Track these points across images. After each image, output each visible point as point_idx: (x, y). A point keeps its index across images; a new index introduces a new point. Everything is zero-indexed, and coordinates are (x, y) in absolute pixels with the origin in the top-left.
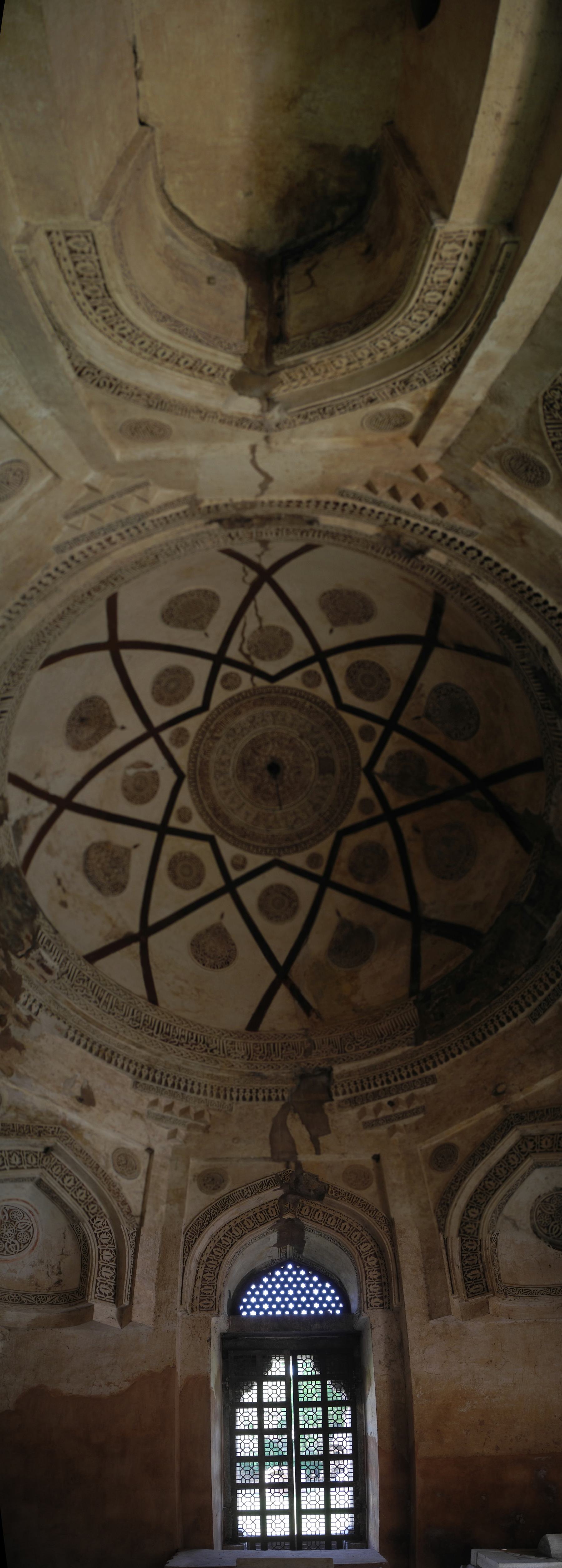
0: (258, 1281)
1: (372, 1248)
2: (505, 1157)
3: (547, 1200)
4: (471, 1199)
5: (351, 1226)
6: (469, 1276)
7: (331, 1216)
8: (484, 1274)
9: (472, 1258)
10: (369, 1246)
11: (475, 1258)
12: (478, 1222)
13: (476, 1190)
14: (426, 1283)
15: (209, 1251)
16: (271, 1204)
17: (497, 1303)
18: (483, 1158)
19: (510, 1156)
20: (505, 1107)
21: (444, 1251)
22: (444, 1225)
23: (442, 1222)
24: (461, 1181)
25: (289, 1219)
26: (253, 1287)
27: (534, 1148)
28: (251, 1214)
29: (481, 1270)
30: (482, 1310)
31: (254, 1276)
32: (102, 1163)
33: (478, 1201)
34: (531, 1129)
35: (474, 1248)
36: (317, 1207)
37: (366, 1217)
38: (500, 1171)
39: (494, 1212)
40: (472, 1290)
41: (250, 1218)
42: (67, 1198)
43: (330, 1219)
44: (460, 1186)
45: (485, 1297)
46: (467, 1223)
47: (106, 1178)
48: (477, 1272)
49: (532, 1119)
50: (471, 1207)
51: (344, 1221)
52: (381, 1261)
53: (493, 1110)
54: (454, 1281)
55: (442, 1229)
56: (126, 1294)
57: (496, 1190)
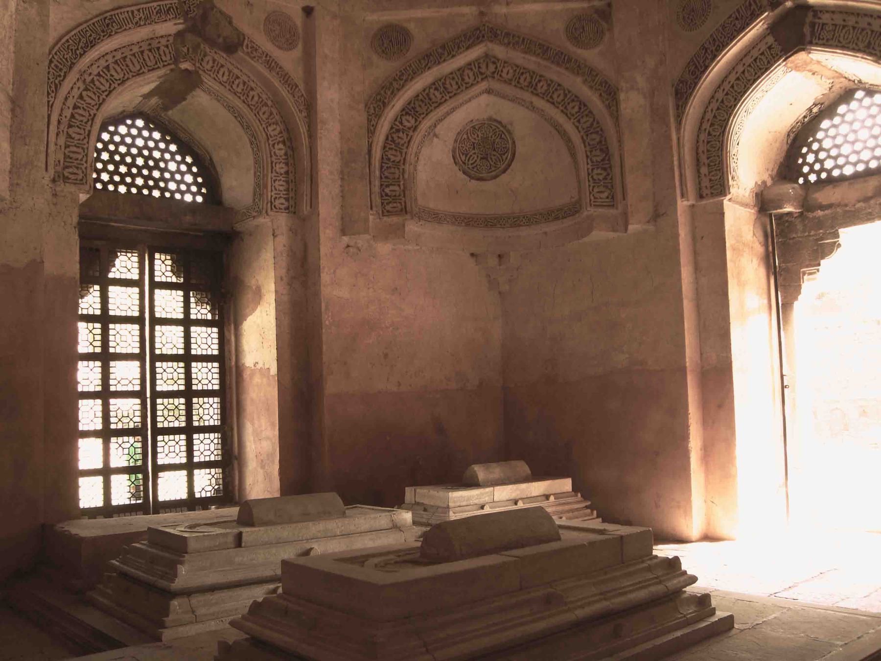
2: (461, 70)
4: (409, 104)
5: (260, 97)
6: (387, 190)
7: (238, 77)
8: (404, 191)
9: (392, 170)
11: (397, 171)
12: (411, 133)
13: (418, 96)
14: (342, 191)
16: (163, 41)
17: (412, 227)
18: (439, 63)
19: (467, 71)
22: (375, 126)
23: (373, 122)
24: (406, 81)
25: (186, 70)
27: (494, 73)
28: (136, 49)
29: (402, 187)
30: (397, 232)
33: (416, 109)
34: (499, 51)
35: (398, 159)
36: (222, 61)
37: (284, 92)
40: (388, 208)
43: (237, 82)
44: (403, 86)
48: (396, 188)
49: (506, 41)
50: (407, 113)
51: (252, 89)
52: (290, 152)
55: (371, 132)
57: (441, 104)
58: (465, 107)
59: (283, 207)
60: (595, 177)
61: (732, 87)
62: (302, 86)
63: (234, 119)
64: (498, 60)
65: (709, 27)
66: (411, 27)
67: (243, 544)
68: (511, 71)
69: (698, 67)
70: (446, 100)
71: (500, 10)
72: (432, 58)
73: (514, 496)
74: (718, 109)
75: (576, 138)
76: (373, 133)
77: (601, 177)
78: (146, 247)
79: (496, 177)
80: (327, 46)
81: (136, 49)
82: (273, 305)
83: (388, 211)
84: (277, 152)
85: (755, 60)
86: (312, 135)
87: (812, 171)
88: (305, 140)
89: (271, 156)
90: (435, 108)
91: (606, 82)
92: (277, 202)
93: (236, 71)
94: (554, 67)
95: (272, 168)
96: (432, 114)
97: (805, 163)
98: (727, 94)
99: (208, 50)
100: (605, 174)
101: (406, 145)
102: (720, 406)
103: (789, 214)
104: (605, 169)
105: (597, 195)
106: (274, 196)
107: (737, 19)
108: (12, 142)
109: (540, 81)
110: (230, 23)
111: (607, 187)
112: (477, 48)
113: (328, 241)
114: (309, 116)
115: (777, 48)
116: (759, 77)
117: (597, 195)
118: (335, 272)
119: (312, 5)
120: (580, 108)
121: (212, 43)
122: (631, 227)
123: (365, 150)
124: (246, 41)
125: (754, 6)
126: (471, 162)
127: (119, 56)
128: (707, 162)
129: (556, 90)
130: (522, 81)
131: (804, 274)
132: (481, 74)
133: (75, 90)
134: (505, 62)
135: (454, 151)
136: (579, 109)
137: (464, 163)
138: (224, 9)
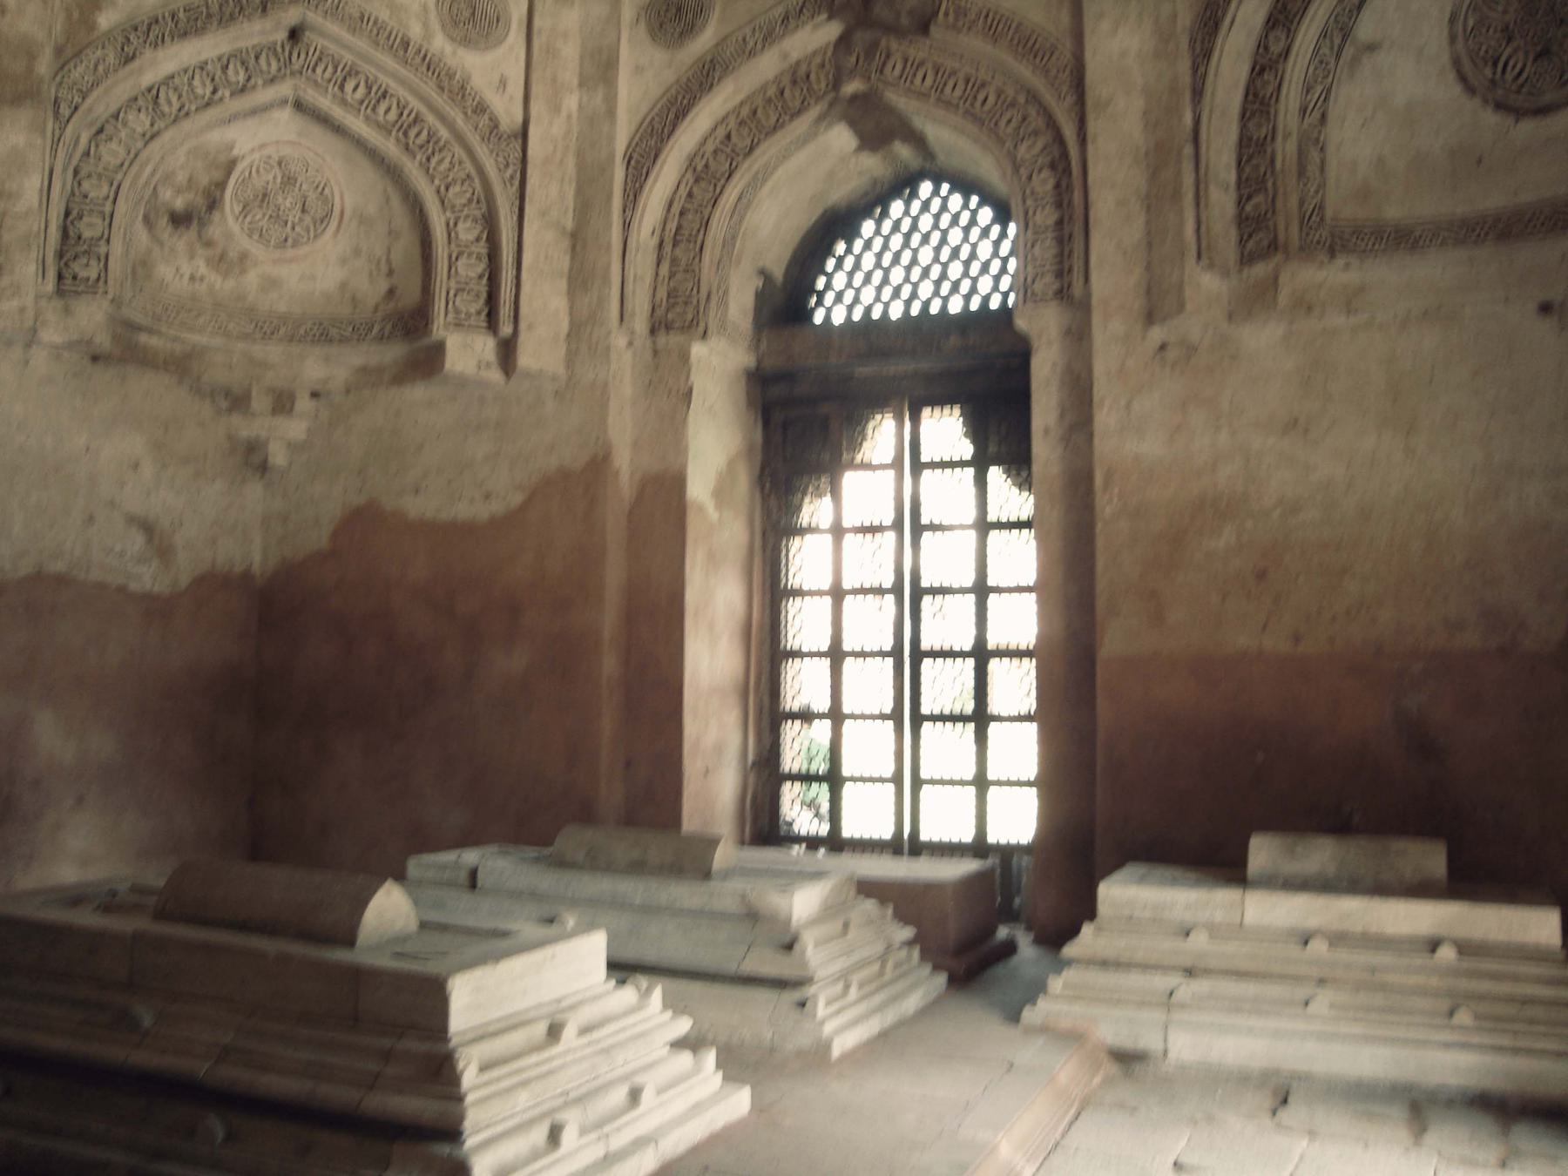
0: (851, 234)
1: (1044, 148)
10: (1040, 144)
15: (683, 192)
21: (1188, 150)
26: (840, 247)
31: (836, 225)
32: (415, 31)
36: (921, 55)
37: (1025, 72)
39: (1324, 34)
41: (770, 101)
42: (357, 125)
43: (951, 84)
47: (430, 65)
54: (1203, 228)
56: (505, 311)
67: (479, 884)
73: (1312, 922)
78: (914, 399)
81: (772, 91)
84: (1039, 189)
89: (1024, 201)
92: (1038, 287)
108: (572, 294)
118: (1128, 406)
126: (1509, 76)
127: (745, 111)
133: (682, 186)
135: (1456, 63)
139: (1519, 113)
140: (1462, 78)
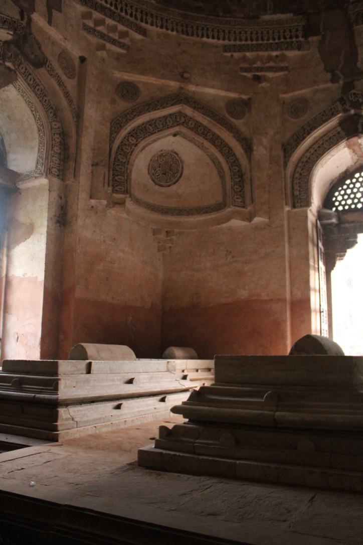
2: (165, 117)
3: (164, 155)
4: (134, 130)
6: (116, 178)
12: (133, 147)
13: (139, 127)
18: (155, 110)
19: (168, 119)
20: (181, 88)
24: (135, 116)
25: (9, 68)
27: (184, 122)
34: (189, 111)
35: (124, 161)
36: (30, 71)
38: (159, 124)
44: (133, 118)
45: (122, 196)
46: (126, 145)
49: (193, 105)
50: (132, 136)
53: (174, 84)
55: (112, 141)
57: (152, 134)
58: (163, 140)
59: (56, 174)
60: (235, 190)
61: (316, 151)
62: (75, 102)
63: (30, 113)
64: (187, 116)
65: (306, 118)
66: (140, 86)
68: (194, 124)
69: (299, 138)
70: (155, 133)
71: (192, 88)
72: (151, 106)
74: (307, 162)
75: (226, 167)
76: (113, 142)
77: (238, 190)
79: (169, 186)
80: (91, 84)
82: (45, 235)
83: (116, 190)
85: (330, 138)
86: (79, 134)
87: (340, 204)
88: (73, 134)
90: (149, 135)
91: (246, 139)
93: (38, 81)
94: (219, 125)
95: (52, 148)
96: (147, 139)
97: (336, 200)
98: (312, 154)
99: (23, 61)
100: (240, 189)
101: (130, 153)
102: (303, 322)
103: (331, 224)
104: (240, 186)
105: (236, 200)
106: (52, 166)
107: (323, 115)
109: (208, 132)
110: (40, 48)
111: (241, 196)
112: (177, 106)
113: (81, 202)
114: (78, 122)
115: (343, 133)
116: (331, 147)
117: (236, 200)
119: (86, 57)
120: (229, 151)
121: (27, 58)
122: (257, 220)
123: (108, 152)
124: (48, 64)
125: (333, 110)
128: (298, 189)
129: (217, 139)
130: (199, 130)
131: (337, 256)
132: (177, 122)
134: (191, 118)
135: (149, 166)
136: (228, 152)
137: (153, 175)
138: (37, 38)
139: (156, 184)
140: (148, 170)
